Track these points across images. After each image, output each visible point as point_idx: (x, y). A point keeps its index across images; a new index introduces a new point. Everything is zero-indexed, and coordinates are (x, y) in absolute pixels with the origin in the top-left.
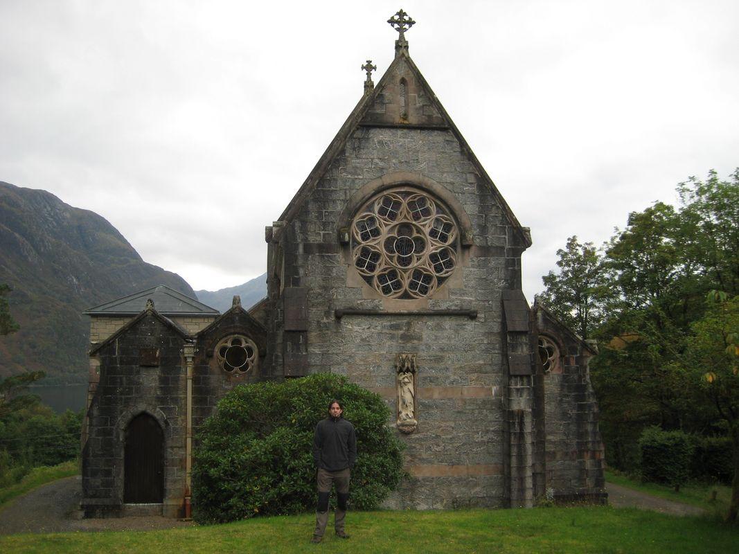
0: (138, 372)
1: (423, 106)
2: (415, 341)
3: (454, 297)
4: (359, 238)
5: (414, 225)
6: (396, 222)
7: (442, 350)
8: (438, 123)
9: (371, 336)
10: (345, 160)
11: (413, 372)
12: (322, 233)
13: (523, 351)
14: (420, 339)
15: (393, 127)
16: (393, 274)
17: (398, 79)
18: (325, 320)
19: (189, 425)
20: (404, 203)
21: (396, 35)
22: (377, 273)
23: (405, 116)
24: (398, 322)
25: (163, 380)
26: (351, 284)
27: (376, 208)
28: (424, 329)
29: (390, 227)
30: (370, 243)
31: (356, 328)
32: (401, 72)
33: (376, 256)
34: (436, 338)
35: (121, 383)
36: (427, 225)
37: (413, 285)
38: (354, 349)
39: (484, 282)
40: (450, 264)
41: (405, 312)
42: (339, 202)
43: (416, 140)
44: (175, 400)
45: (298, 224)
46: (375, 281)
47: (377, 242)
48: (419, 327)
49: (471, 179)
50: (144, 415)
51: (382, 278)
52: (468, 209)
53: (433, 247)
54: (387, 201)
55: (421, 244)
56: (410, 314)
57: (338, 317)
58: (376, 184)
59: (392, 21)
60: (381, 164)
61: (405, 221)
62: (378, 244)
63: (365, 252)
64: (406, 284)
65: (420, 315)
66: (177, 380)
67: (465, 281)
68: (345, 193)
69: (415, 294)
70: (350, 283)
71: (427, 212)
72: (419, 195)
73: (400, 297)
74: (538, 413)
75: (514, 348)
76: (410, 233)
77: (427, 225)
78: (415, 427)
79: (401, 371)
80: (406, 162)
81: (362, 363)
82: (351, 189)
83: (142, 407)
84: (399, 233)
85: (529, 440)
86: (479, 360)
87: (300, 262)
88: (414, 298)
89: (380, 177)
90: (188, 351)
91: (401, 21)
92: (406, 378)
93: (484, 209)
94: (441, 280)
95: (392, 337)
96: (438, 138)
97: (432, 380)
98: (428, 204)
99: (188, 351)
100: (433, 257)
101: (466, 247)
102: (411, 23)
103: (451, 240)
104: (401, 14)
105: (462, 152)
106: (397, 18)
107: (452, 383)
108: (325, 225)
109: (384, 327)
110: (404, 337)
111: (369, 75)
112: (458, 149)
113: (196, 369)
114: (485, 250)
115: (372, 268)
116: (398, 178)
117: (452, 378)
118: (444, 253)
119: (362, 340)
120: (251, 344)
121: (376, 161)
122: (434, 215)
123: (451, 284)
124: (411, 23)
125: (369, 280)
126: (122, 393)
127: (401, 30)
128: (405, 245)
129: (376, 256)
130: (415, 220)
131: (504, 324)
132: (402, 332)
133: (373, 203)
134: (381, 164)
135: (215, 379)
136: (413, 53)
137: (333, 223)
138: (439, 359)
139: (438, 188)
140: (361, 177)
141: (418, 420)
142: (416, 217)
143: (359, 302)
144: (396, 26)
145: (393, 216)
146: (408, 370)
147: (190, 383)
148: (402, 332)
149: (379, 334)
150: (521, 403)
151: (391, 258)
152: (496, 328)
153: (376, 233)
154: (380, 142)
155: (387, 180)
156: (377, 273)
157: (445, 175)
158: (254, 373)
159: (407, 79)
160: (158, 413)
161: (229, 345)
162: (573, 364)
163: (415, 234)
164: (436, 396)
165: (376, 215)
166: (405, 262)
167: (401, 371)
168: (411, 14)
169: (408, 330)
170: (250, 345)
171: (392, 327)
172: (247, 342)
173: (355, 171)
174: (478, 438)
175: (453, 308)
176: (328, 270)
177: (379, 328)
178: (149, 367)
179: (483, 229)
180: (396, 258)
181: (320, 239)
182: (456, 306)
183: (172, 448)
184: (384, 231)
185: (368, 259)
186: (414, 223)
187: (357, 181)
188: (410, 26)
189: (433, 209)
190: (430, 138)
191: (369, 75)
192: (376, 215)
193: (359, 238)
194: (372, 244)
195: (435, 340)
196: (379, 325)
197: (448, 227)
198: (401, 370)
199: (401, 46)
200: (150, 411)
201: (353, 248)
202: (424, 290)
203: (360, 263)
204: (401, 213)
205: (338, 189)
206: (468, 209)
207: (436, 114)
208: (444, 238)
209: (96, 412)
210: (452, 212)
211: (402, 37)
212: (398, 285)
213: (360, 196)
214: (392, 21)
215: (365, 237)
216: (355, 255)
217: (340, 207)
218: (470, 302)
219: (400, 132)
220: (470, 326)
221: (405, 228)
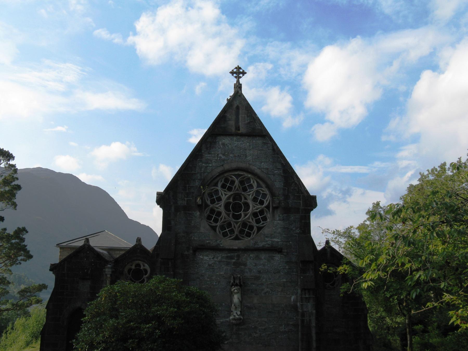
1: (250, 122)
2: (243, 267)
3: (267, 239)
4: (209, 202)
5: (243, 194)
6: (232, 193)
7: (259, 272)
11: (241, 286)
12: (186, 199)
14: (245, 265)
15: (231, 135)
16: (229, 225)
17: (235, 106)
18: (186, 253)
20: (237, 183)
21: (235, 81)
23: (238, 128)
24: (232, 254)
26: (203, 230)
27: (220, 185)
28: (250, 260)
29: (227, 196)
30: (215, 206)
31: (206, 258)
32: (236, 103)
33: (219, 214)
34: (256, 265)
37: (241, 232)
38: (204, 271)
41: (236, 248)
42: (197, 181)
43: (245, 143)
47: (220, 204)
49: (279, 166)
51: (222, 228)
53: (253, 207)
54: (226, 180)
56: (239, 250)
58: (220, 169)
59: (232, 73)
60: (223, 157)
61: (236, 192)
63: (212, 211)
65: (247, 250)
67: (274, 229)
68: (201, 175)
69: (243, 237)
70: (202, 230)
78: (241, 321)
79: (233, 285)
80: (238, 156)
81: (208, 280)
82: (204, 172)
84: (234, 199)
86: (283, 279)
88: (241, 239)
89: (223, 165)
90: (108, 270)
92: (234, 289)
94: (259, 229)
95: (228, 264)
96: (259, 141)
98: (252, 182)
99: (108, 270)
100: (255, 215)
103: (266, 204)
105: (274, 150)
107: (265, 293)
110: (235, 264)
112: (271, 148)
114: (287, 210)
115: (216, 221)
116: (234, 165)
117: (266, 290)
118: (262, 212)
119: (209, 265)
120: (147, 267)
121: (220, 155)
123: (266, 231)
124: (244, 73)
125: (214, 228)
128: (236, 206)
130: (244, 191)
132: (234, 261)
133: (218, 182)
134: (223, 157)
136: (244, 92)
137: (193, 193)
138: (257, 278)
139: (258, 171)
140: (211, 165)
141: (243, 316)
143: (207, 242)
145: (230, 189)
146: (237, 285)
148: (234, 261)
149: (220, 262)
150: (310, 307)
151: (228, 215)
154: (223, 144)
155: (227, 167)
157: (263, 164)
159: (240, 106)
161: (133, 267)
164: (255, 301)
166: (237, 217)
167: (233, 285)
169: (238, 259)
170: (145, 267)
171: (227, 257)
172: (144, 266)
175: (267, 246)
177: (219, 258)
180: (231, 215)
181: (185, 203)
182: (269, 245)
184: (224, 198)
185: (213, 215)
186: (243, 193)
187: (208, 168)
188: (243, 75)
189: (255, 185)
190: (254, 141)
192: (219, 188)
193: (209, 202)
194: (217, 206)
195: (255, 266)
196: (220, 256)
197: (264, 196)
198: (235, 285)
199: (238, 87)
201: (205, 208)
202: (248, 235)
203: (209, 218)
204: (235, 187)
205: (196, 172)
206: (278, 184)
211: (238, 81)
212: (232, 231)
214: (232, 73)
215: (213, 202)
216: (207, 212)
218: (278, 242)
219: (235, 138)
220: (277, 257)
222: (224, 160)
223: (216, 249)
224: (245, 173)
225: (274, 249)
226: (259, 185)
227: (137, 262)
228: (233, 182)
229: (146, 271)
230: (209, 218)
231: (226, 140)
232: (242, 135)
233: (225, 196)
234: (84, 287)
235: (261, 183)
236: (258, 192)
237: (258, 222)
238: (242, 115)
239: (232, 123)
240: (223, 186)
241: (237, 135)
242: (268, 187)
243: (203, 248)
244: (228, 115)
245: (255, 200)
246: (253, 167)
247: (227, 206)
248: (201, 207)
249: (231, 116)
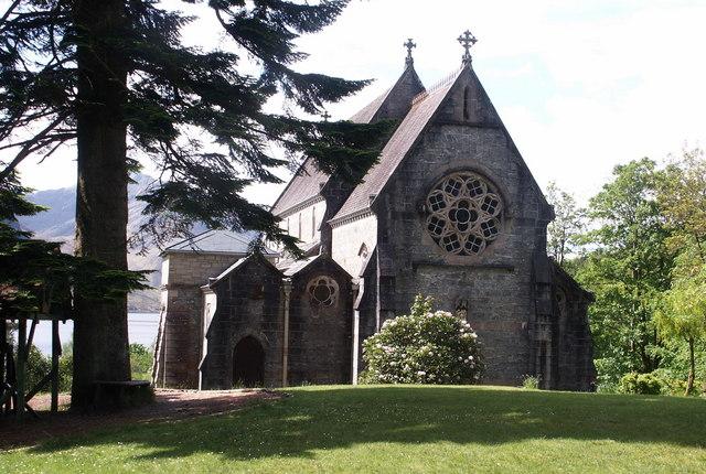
0: (246, 303)
4: (431, 208)
6: (458, 198)
7: (488, 294)
8: (490, 123)
9: (438, 283)
10: (423, 149)
13: (547, 297)
14: (472, 285)
15: (458, 124)
16: (454, 237)
19: (286, 346)
22: (443, 235)
23: (466, 115)
25: (266, 310)
27: (444, 187)
28: (476, 279)
31: (428, 276)
32: (465, 84)
33: (442, 223)
35: (233, 311)
36: (479, 200)
37: (468, 246)
39: (519, 245)
40: (494, 231)
44: (275, 326)
45: (388, 196)
46: (442, 241)
48: (471, 276)
49: (514, 167)
50: (250, 337)
51: (446, 240)
52: (511, 189)
53: (483, 217)
54: (452, 182)
55: (475, 216)
57: (416, 266)
59: (460, 39)
60: (449, 153)
62: (443, 214)
63: (435, 220)
64: (463, 246)
65: (473, 268)
66: (276, 310)
67: (506, 242)
70: (424, 242)
71: (480, 191)
72: (478, 179)
73: (460, 254)
74: (554, 344)
75: (540, 294)
76: (467, 207)
77: (479, 200)
83: (248, 331)
85: (549, 361)
87: (389, 225)
91: (467, 40)
93: (521, 190)
94: (488, 243)
96: (491, 134)
97: (482, 316)
100: (484, 225)
101: (507, 219)
102: (474, 41)
103: (496, 213)
104: (467, 33)
105: (508, 146)
106: (464, 36)
108: (407, 198)
109: (447, 276)
111: (410, 51)
113: (291, 302)
114: (521, 221)
115: (439, 231)
116: (462, 164)
118: (491, 223)
120: (335, 284)
122: (485, 194)
123: (496, 245)
125: (437, 241)
126: (234, 320)
127: (466, 46)
128: (462, 215)
129: (442, 223)
131: (533, 277)
134: (449, 153)
135: (306, 310)
138: (486, 301)
139: (489, 173)
142: (472, 194)
144: (464, 43)
146: (464, 308)
147: (287, 312)
150: (544, 335)
152: (526, 280)
153: (443, 205)
154: (449, 136)
155: (453, 166)
156: (443, 235)
158: (336, 305)
160: (261, 336)
162: (576, 309)
163: (471, 208)
165: (443, 192)
168: (475, 34)
173: (430, 158)
174: (511, 359)
176: (410, 232)
178: (255, 298)
179: (521, 205)
181: (403, 209)
183: (271, 363)
184: (449, 204)
189: (485, 189)
191: (410, 51)
192: (443, 192)
196: (443, 275)
197: (495, 203)
199: (467, 60)
200: (255, 333)
203: (431, 228)
206: (511, 189)
207: (490, 116)
208: (491, 211)
209: (212, 334)
210: (499, 191)
211: (467, 52)
212: (457, 245)
213: (433, 176)
214: (460, 39)
217: (418, 185)
220: (508, 277)
221: (464, 203)
222: (449, 157)
223: (439, 265)
224: (469, 174)
225: (506, 268)
226: (489, 191)
227: (323, 277)
228: (459, 185)
229: (333, 289)
230: (431, 228)
231: (452, 131)
232: (472, 126)
233: (451, 201)
234: (256, 309)
235: (492, 186)
236: (487, 200)
237: (487, 234)
238: (473, 100)
239: (460, 109)
240: (448, 190)
241: (466, 124)
242: (499, 191)
243: (425, 264)
244: (455, 98)
245: (484, 207)
246: (483, 168)
247: (451, 214)
248: (424, 215)
249: (459, 99)
